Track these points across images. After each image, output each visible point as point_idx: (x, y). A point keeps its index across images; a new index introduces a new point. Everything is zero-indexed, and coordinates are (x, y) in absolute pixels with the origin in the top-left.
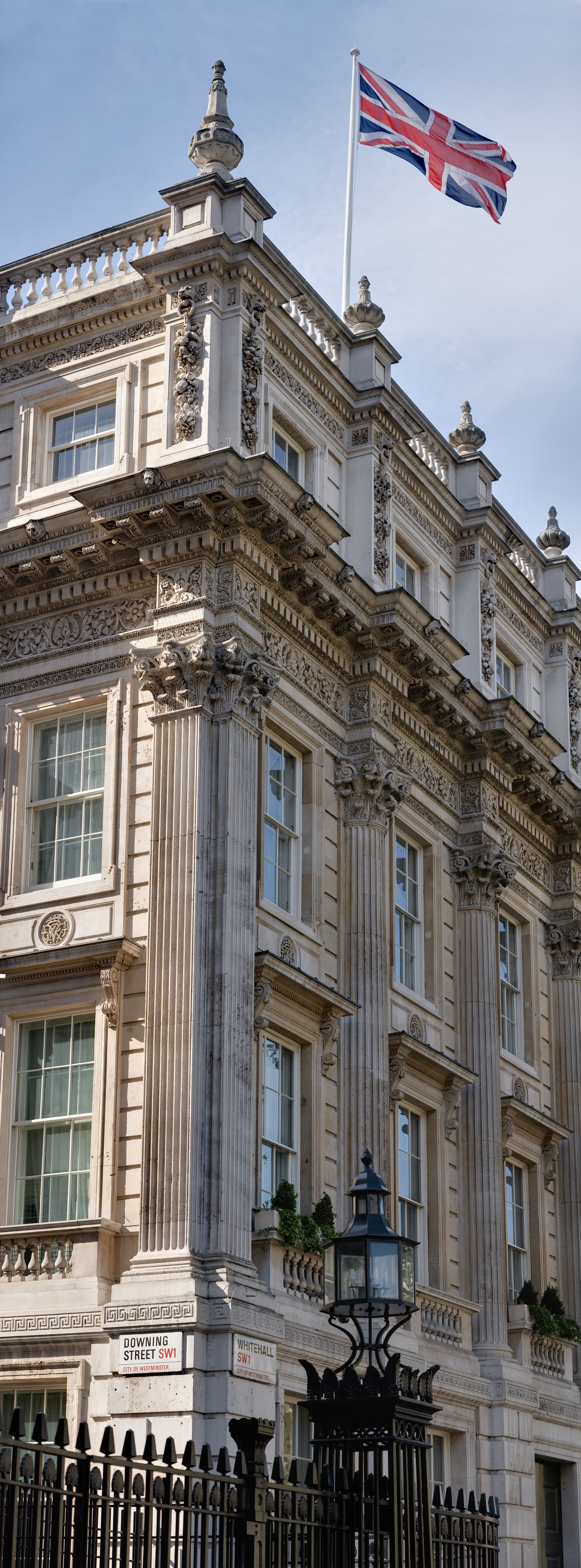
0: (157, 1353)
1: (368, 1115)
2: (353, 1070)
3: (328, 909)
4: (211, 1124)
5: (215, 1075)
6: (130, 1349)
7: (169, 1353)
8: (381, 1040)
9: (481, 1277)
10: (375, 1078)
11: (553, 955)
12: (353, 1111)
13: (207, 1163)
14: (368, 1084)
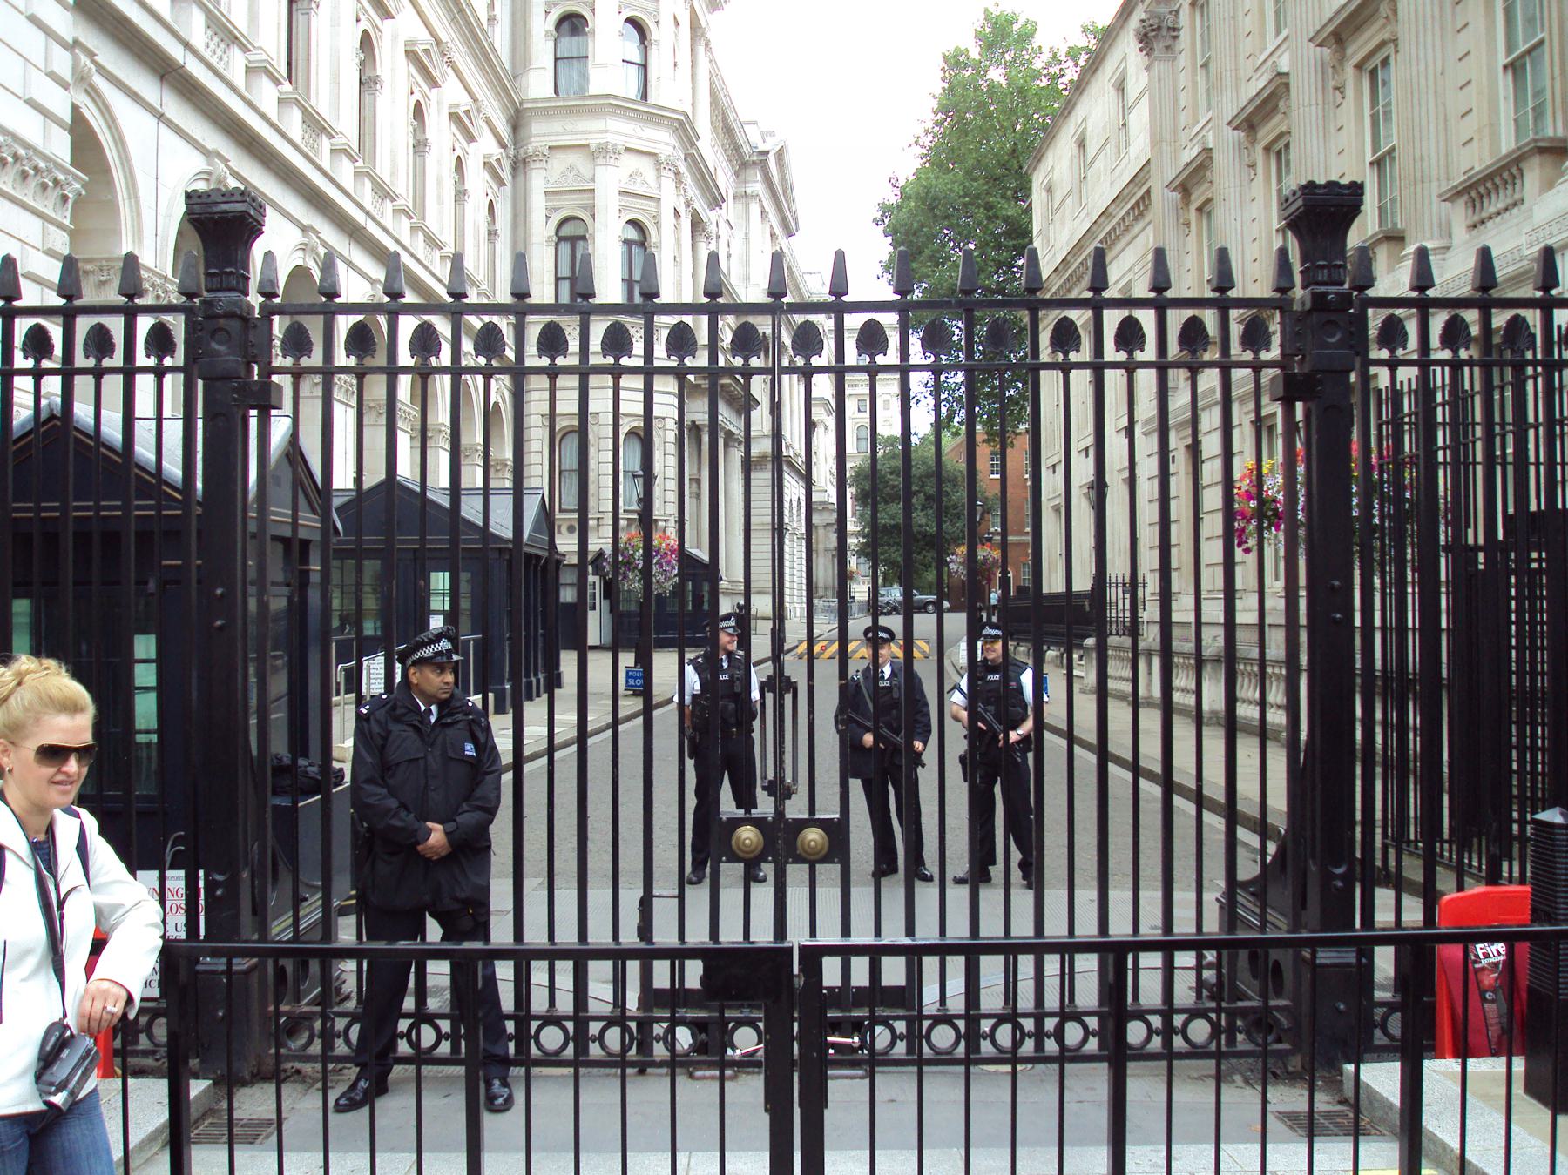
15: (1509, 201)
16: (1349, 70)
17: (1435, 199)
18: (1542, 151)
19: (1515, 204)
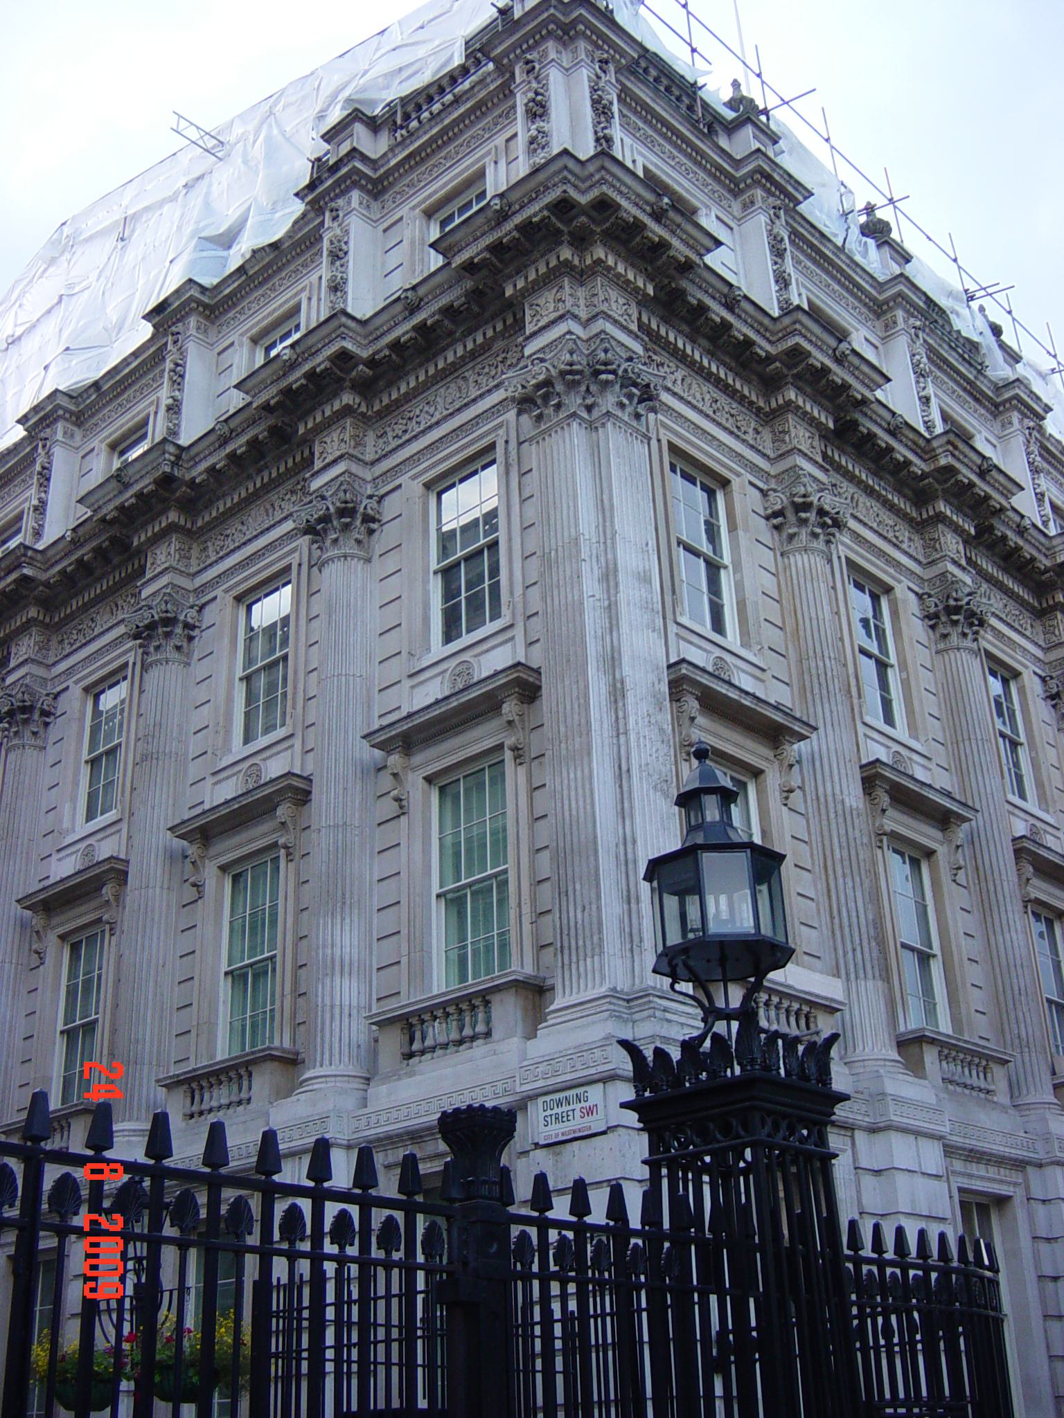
0: (577, 1113)
1: (844, 844)
2: (822, 799)
3: (772, 636)
4: (625, 844)
5: (625, 789)
6: (549, 1112)
7: (590, 1111)
8: (848, 765)
9: (1014, 1026)
10: (847, 805)
11: (1054, 706)
12: (827, 843)
13: (625, 888)
14: (840, 812)
15: (235, 1098)
16: (52, 938)
17: (153, 1083)
19: (240, 1103)
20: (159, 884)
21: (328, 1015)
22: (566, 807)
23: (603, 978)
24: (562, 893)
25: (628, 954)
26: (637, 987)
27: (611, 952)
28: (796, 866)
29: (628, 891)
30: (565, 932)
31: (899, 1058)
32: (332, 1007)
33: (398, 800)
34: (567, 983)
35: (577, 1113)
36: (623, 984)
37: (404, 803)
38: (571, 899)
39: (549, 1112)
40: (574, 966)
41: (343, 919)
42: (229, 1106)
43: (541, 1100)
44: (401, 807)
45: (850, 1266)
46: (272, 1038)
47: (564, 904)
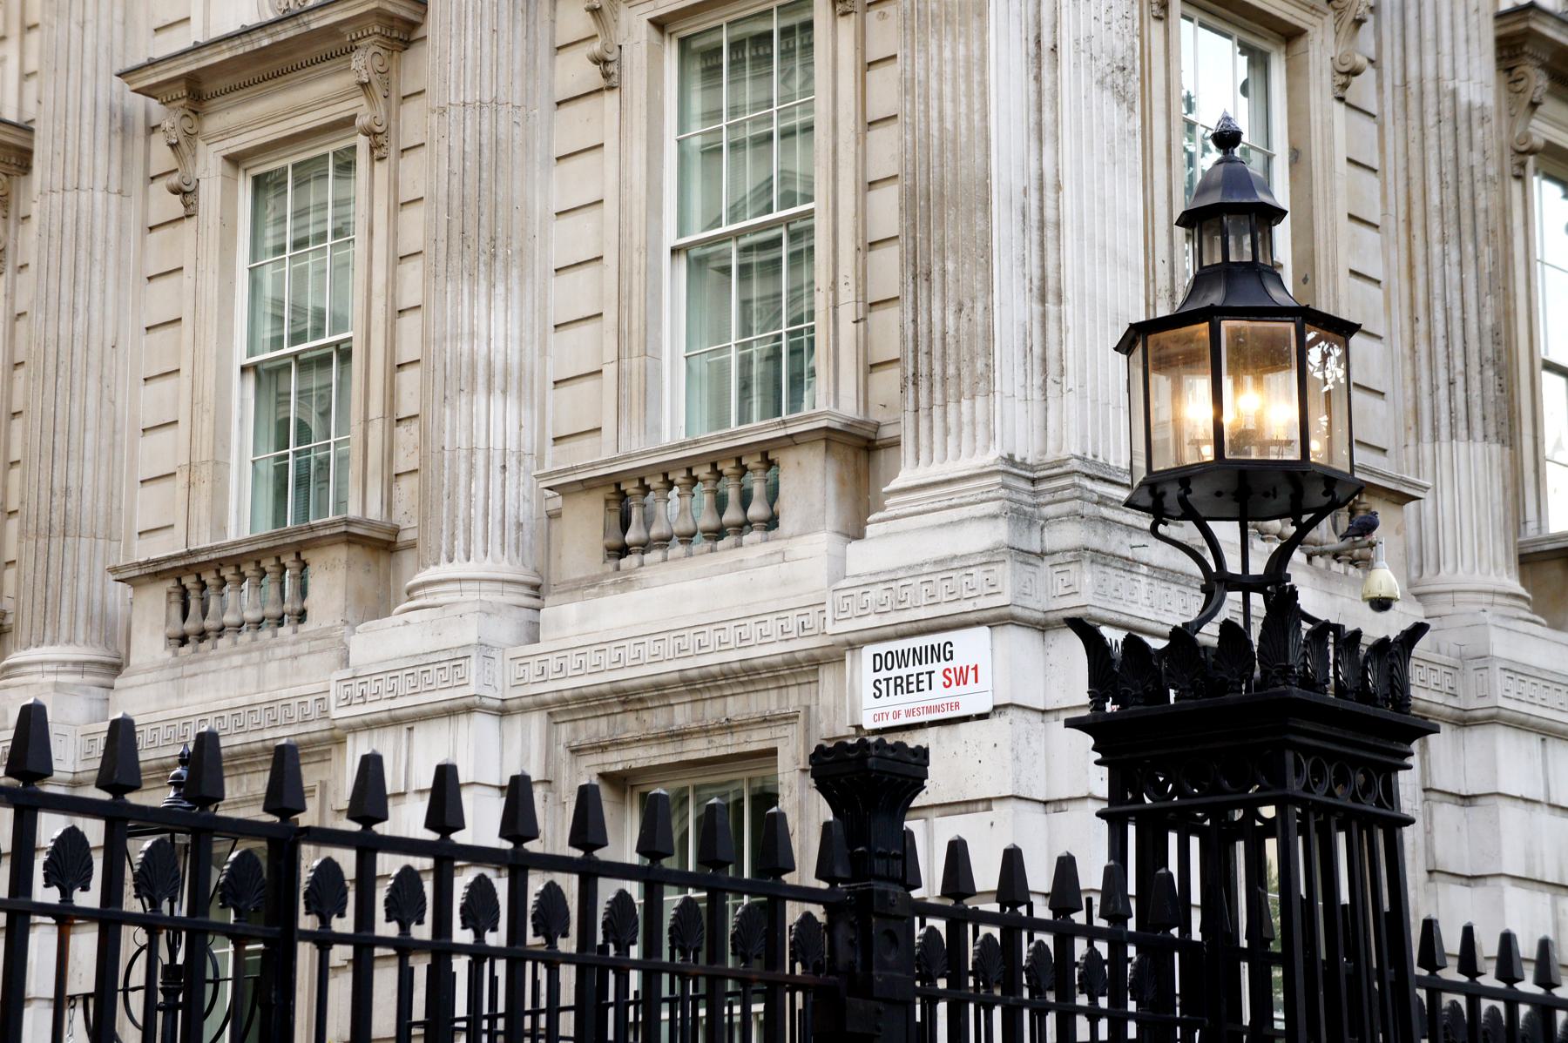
0: (938, 679)
1: (1449, 178)
4: (1041, 188)
7: (961, 677)
8: (1473, 19)
13: (1036, 273)
14: (1447, 114)
18: (351, 539)
20: (100, 184)
21: (463, 468)
22: (934, 114)
23: (991, 437)
24: (919, 273)
25: (1037, 395)
26: (1050, 456)
27: (1007, 390)
28: (1351, 217)
29: (1043, 279)
30: (923, 348)
31: (1522, 591)
32: (472, 451)
33: (601, 61)
34: (924, 441)
35: (938, 679)
36: (1027, 450)
37: (612, 68)
38: (937, 285)
39: (884, 674)
40: (937, 412)
41: (492, 286)
42: (258, 624)
43: (868, 651)
44: (606, 76)
45: (1422, 993)
46: (341, 503)
47: (923, 295)
